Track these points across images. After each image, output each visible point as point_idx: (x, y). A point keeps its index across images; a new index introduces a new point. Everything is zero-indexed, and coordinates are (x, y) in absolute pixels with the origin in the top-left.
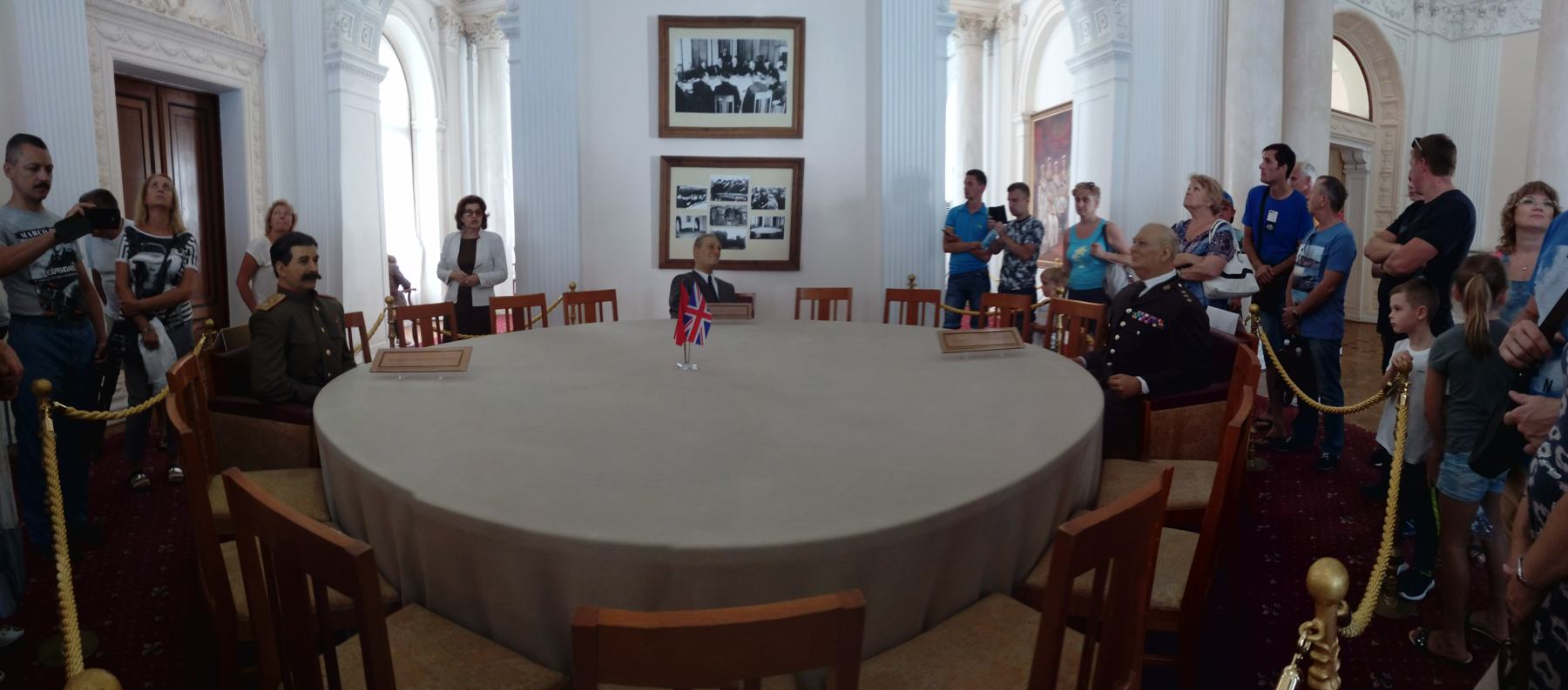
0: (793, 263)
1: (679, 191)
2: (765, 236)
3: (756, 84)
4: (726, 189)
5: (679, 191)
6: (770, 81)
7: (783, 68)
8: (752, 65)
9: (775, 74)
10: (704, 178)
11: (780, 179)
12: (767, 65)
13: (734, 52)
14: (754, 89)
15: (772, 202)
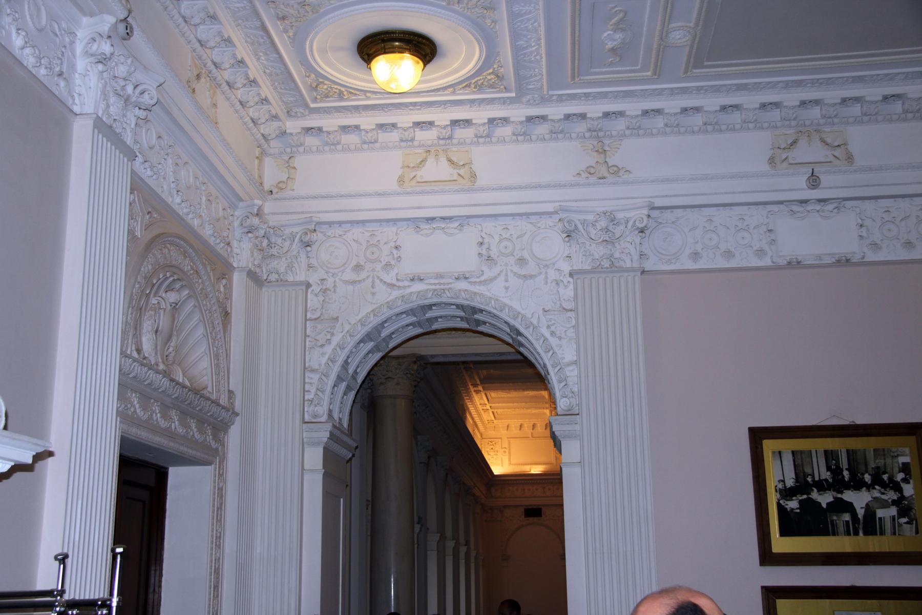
6: (891, 495)
7: (905, 480)
8: (867, 478)
9: (897, 488)
12: (885, 477)
13: (844, 463)
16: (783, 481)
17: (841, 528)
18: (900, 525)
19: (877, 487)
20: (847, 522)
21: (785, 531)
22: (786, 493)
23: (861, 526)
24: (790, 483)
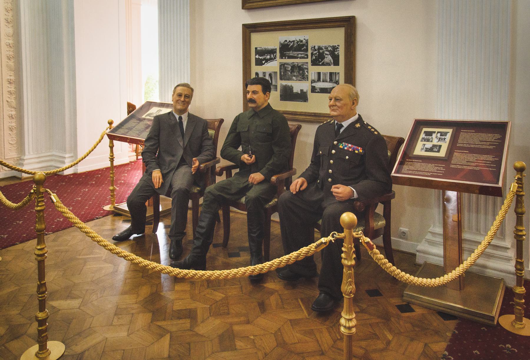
1: (258, 52)
4: (292, 49)
11: (335, 37)
15: (329, 58)
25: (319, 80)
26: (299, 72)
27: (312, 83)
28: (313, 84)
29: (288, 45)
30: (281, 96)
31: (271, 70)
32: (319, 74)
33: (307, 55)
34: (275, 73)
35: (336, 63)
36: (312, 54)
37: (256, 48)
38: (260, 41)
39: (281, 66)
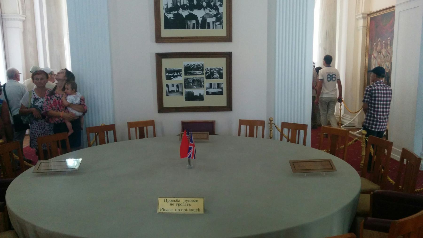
0: (229, 107)
1: (167, 71)
2: (214, 93)
3: (207, 14)
5: (167, 71)
6: (214, 12)
8: (204, 4)
9: (217, 9)
10: (180, 64)
11: (221, 63)
12: (212, 4)
14: (206, 16)
15: (217, 75)
16: (167, 5)
17: (191, 26)
18: (216, 25)
19: (208, 8)
20: (194, 24)
21: (166, 28)
22: (168, 10)
23: (200, 26)
24: (170, 5)
25: (211, 87)
26: (197, 83)
27: (206, 89)
28: (207, 90)
29: (190, 67)
30: (185, 98)
31: (178, 83)
32: (211, 84)
33: (203, 73)
34: (181, 84)
35: (221, 77)
36: (206, 73)
37: (166, 69)
38: (168, 64)
39: (185, 80)
